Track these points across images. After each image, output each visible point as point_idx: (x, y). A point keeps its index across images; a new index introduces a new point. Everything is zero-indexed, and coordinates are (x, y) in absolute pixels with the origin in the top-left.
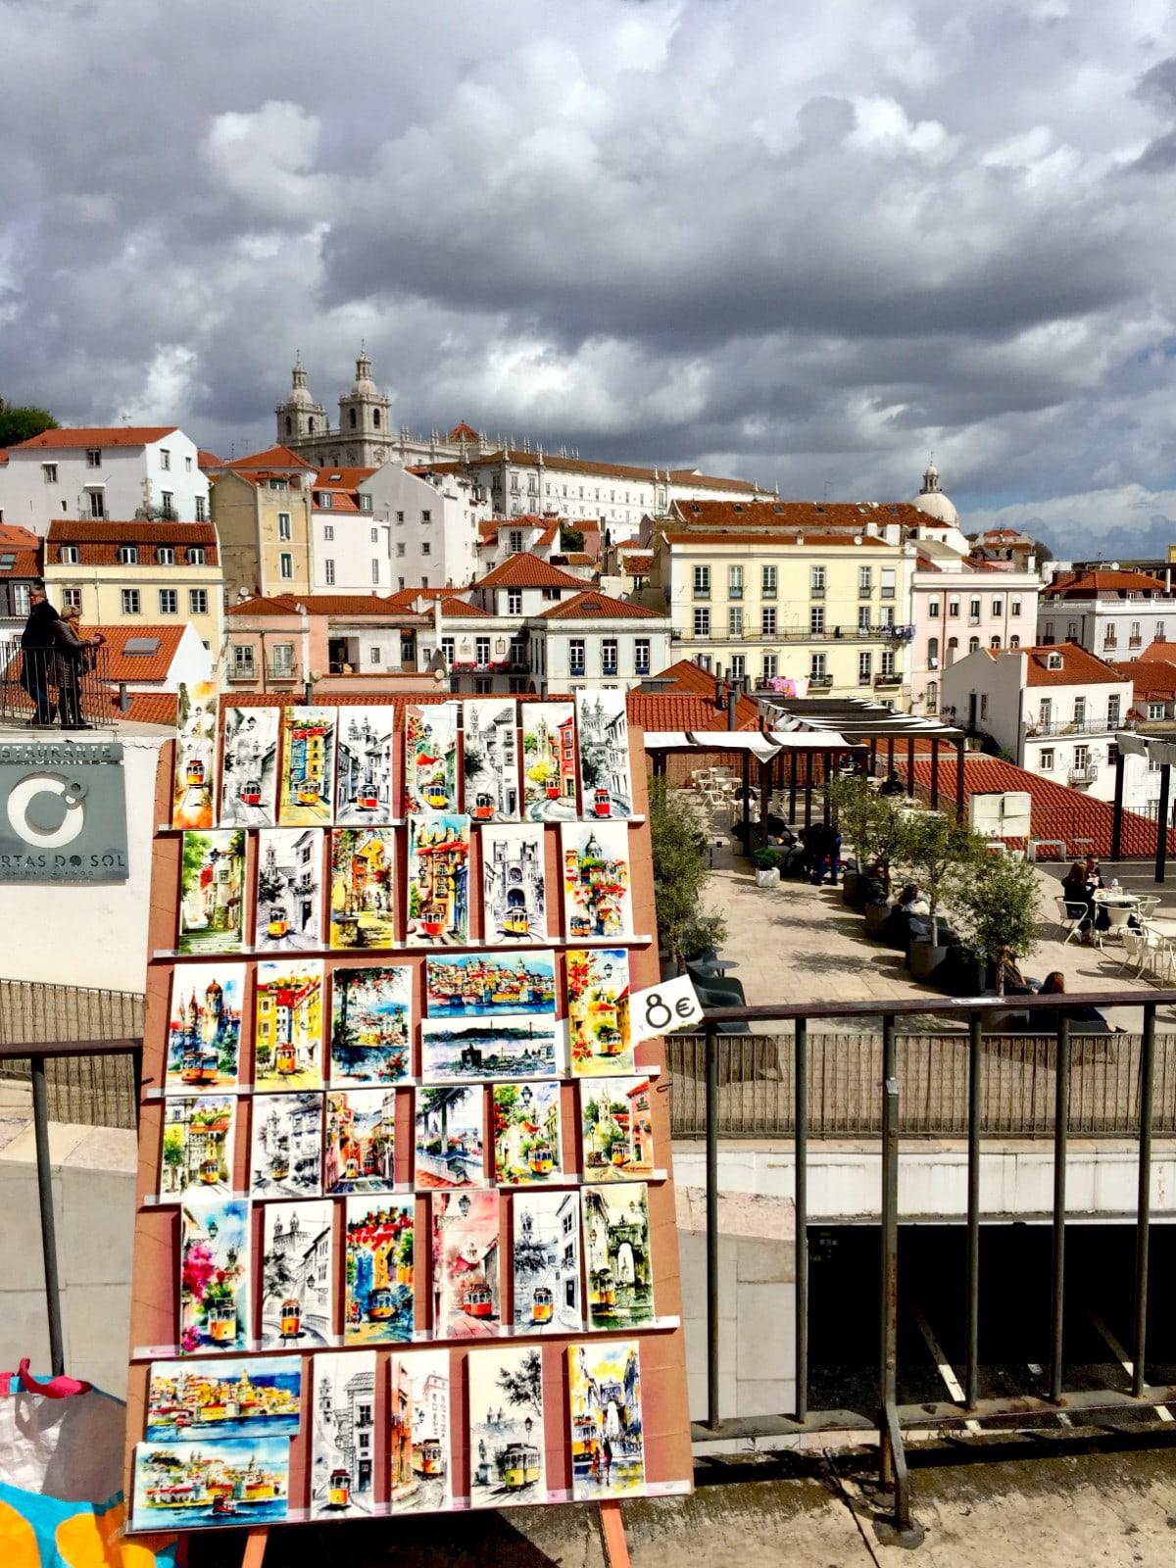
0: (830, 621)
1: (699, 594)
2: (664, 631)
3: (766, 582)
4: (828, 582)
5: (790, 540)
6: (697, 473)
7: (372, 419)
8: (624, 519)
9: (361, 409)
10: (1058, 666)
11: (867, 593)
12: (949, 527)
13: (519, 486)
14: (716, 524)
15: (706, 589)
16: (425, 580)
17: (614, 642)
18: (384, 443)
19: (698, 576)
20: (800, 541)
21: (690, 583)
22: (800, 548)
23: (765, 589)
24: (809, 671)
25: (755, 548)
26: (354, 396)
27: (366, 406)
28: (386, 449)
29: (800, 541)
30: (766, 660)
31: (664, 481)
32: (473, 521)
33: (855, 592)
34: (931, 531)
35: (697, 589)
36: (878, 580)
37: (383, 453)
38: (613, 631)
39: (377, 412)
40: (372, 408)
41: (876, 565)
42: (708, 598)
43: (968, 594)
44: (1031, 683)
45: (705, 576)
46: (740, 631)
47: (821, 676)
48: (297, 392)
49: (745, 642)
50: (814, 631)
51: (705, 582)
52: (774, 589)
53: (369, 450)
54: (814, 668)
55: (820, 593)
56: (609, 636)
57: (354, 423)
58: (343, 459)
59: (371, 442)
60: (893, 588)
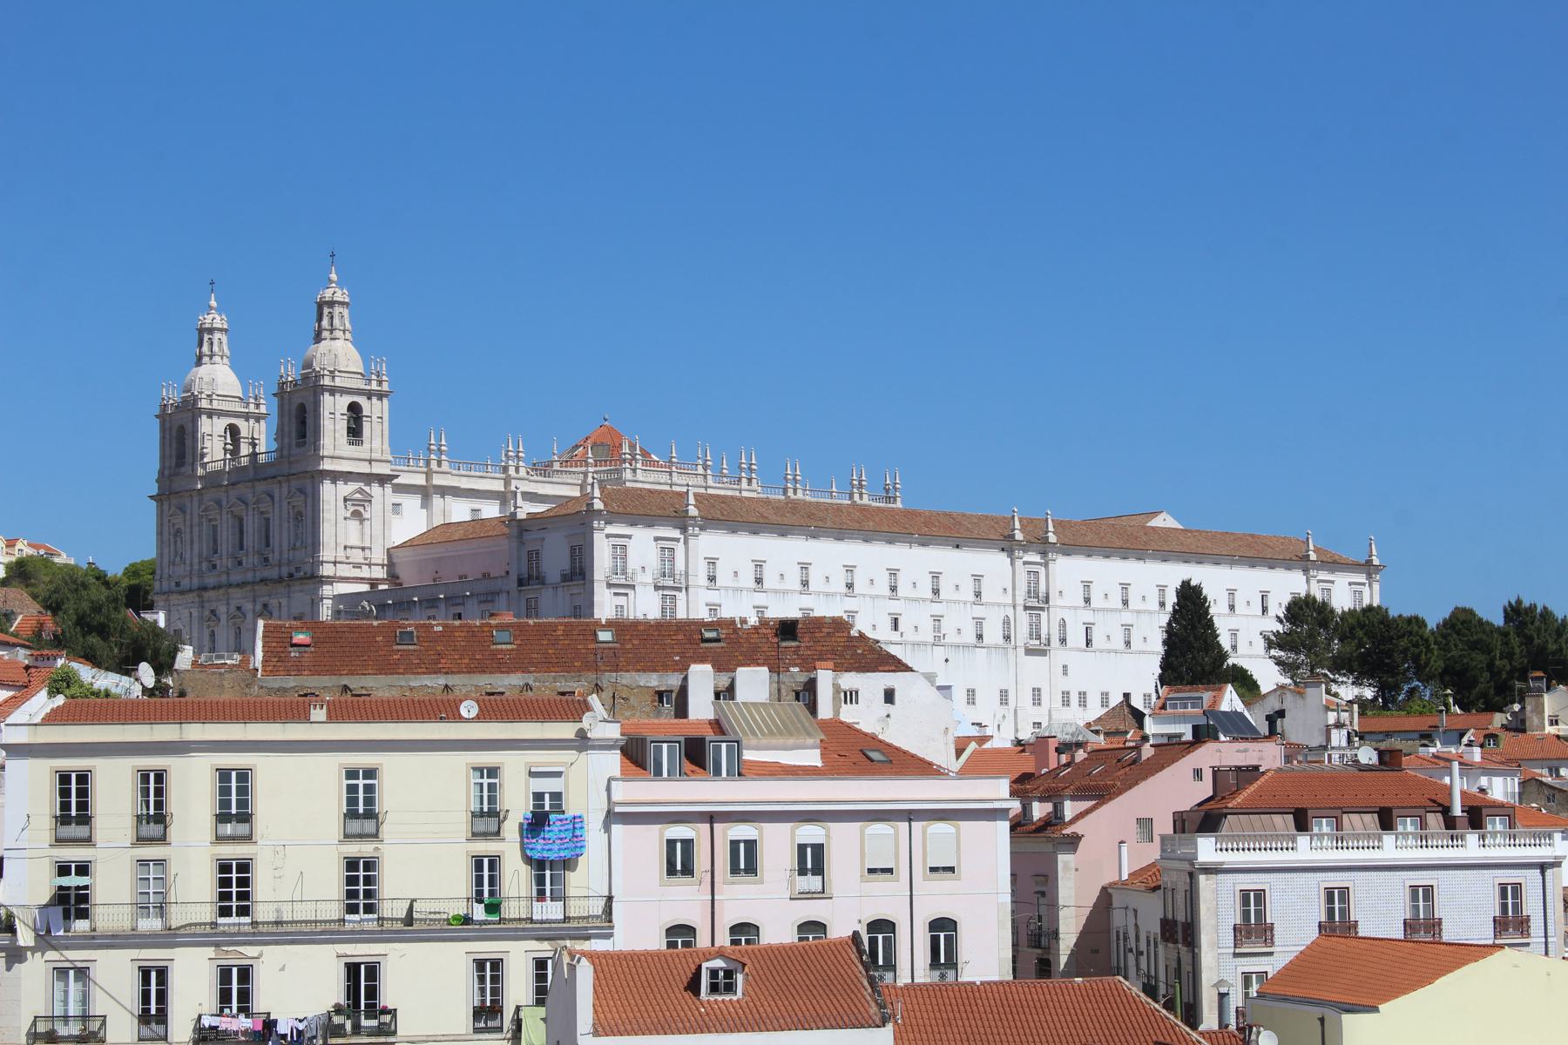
0: (394, 890)
3: (225, 804)
4: (387, 801)
6: (1164, 521)
7: (342, 425)
9: (317, 405)
10: (730, 988)
11: (492, 825)
12: (908, 669)
13: (633, 563)
14: (332, 671)
18: (369, 478)
20: (319, 714)
21: (45, 802)
22: (319, 728)
23: (223, 818)
25: (195, 732)
26: (305, 378)
27: (327, 399)
28: (375, 490)
29: (319, 714)
30: (225, 974)
31: (1041, 545)
33: (460, 824)
34: (849, 680)
37: (369, 500)
39: (354, 409)
40: (347, 400)
41: (513, 765)
42: (88, 841)
43: (784, 828)
44: (599, 1030)
45: (83, 793)
46: (161, 909)
47: (373, 1010)
48: (204, 371)
49: (171, 938)
50: (352, 909)
52: (245, 817)
53: (331, 495)
54: (353, 991)
55: (369, 826)
57: (302, 435)
59: (335, 476)
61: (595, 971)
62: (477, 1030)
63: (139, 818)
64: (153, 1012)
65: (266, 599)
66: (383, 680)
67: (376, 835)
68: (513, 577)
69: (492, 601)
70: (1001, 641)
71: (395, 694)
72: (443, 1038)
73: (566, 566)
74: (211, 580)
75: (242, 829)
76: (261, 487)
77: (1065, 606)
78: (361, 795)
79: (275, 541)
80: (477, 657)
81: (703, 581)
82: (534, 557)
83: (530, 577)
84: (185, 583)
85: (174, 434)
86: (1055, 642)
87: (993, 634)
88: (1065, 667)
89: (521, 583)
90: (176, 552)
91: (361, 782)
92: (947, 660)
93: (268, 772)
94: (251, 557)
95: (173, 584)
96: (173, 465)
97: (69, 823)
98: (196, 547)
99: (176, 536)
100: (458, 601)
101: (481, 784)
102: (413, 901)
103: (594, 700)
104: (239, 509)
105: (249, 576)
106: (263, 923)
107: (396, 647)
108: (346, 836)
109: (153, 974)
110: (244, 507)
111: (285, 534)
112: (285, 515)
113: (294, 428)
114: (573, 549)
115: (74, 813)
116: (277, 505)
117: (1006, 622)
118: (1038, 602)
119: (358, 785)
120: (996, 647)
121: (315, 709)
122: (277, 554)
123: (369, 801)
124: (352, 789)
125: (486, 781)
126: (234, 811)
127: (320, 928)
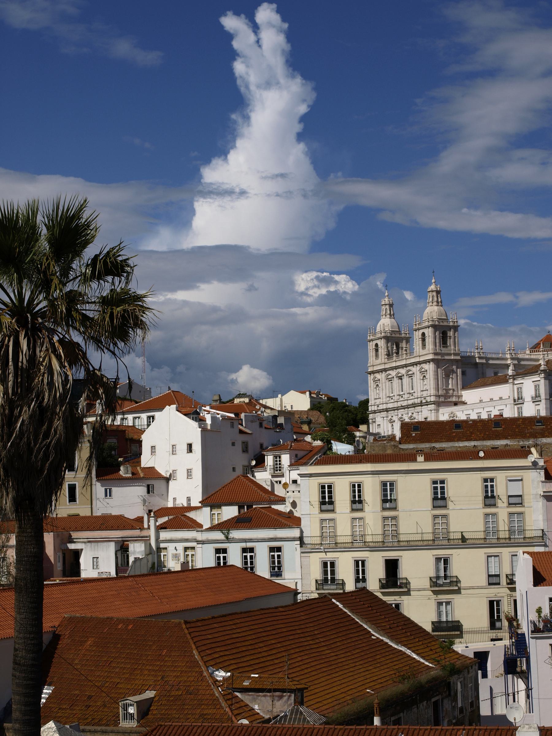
1: (324, 507)
2: (293, 539)
4: (450, 492)
5: (413, 458)
15: (331, 503)
16: (189, 499)
17: (252, 550)
19: (323, 492)
20: (420, 458)
21: (316, 497)
22: (420, 463)
23: (385, 501)
24: (433, 574)
32: (245, 450)
35: (323, 503)
36: (501, 490)
38: (251, 540)
45: (330, 492)
51: (330, 497)
56: (244, 545)
58: (418, 376)
60: (520, 496)
61: (533, 561)
62: (490, 584)
63: (353, 502)
64: (361, 578)
65: (413, 411)
66: (450, 444)
67: (445, 507)
68: (512, 398)
71: (454, 450)
72: (476, 588)
73: (533, 394)
74: (390, 406)
75: (392, 505)
76: (408, 368)
78: (439, 491)
79: (415, 388)
80: (487, 433)
82: (520, 391)
83: (518, 399)
84: (381, 407)
85: (374, 347)
89: (515, 401)
91: (439, 485)
93: (402, 482)
94: (406, 394)
95: (376, 406)
96: (374, 359)
97: (325, 504)
98: (384, 391)
101: (487, 485)
102: (462, 532)
103: (533, 450)
105: (405, 403)
106: (402, 541)
107: (454, 431)
108: (434, 507)
109: (360, 562)
111: (419, 385)
112: (418, 377)
113: (421, 342)
114: (536, 386)
115: (327, 500)
116: (415, 373)
119: (437, 487)
121: (419, 456)
122: (416, 393)
123: (443, 493)
124: (435, 488)
125: (489, 484)
126: (389, 498)
127: (425, 543)
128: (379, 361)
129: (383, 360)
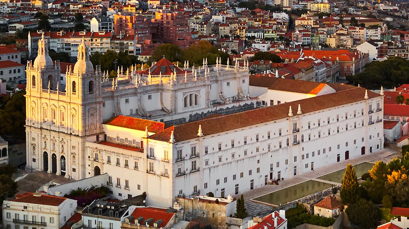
8: (266, 150)
13: (183, 155)
69: (138, 160)
70: (286, 145)
77: (304, 132)
81: (204, 153)
86: (301, 142)
87: (284, 145)
88: (303, 148)
90: (33, 114)
92: (271, 156)
99: (33, 109)
100: (127, 156)
104: (53, 107)
110: (55, 108)
117: (288, 140)
118: (296, 130)
120: (285, 148)
128: (36, 89)
129: (39, 91)
